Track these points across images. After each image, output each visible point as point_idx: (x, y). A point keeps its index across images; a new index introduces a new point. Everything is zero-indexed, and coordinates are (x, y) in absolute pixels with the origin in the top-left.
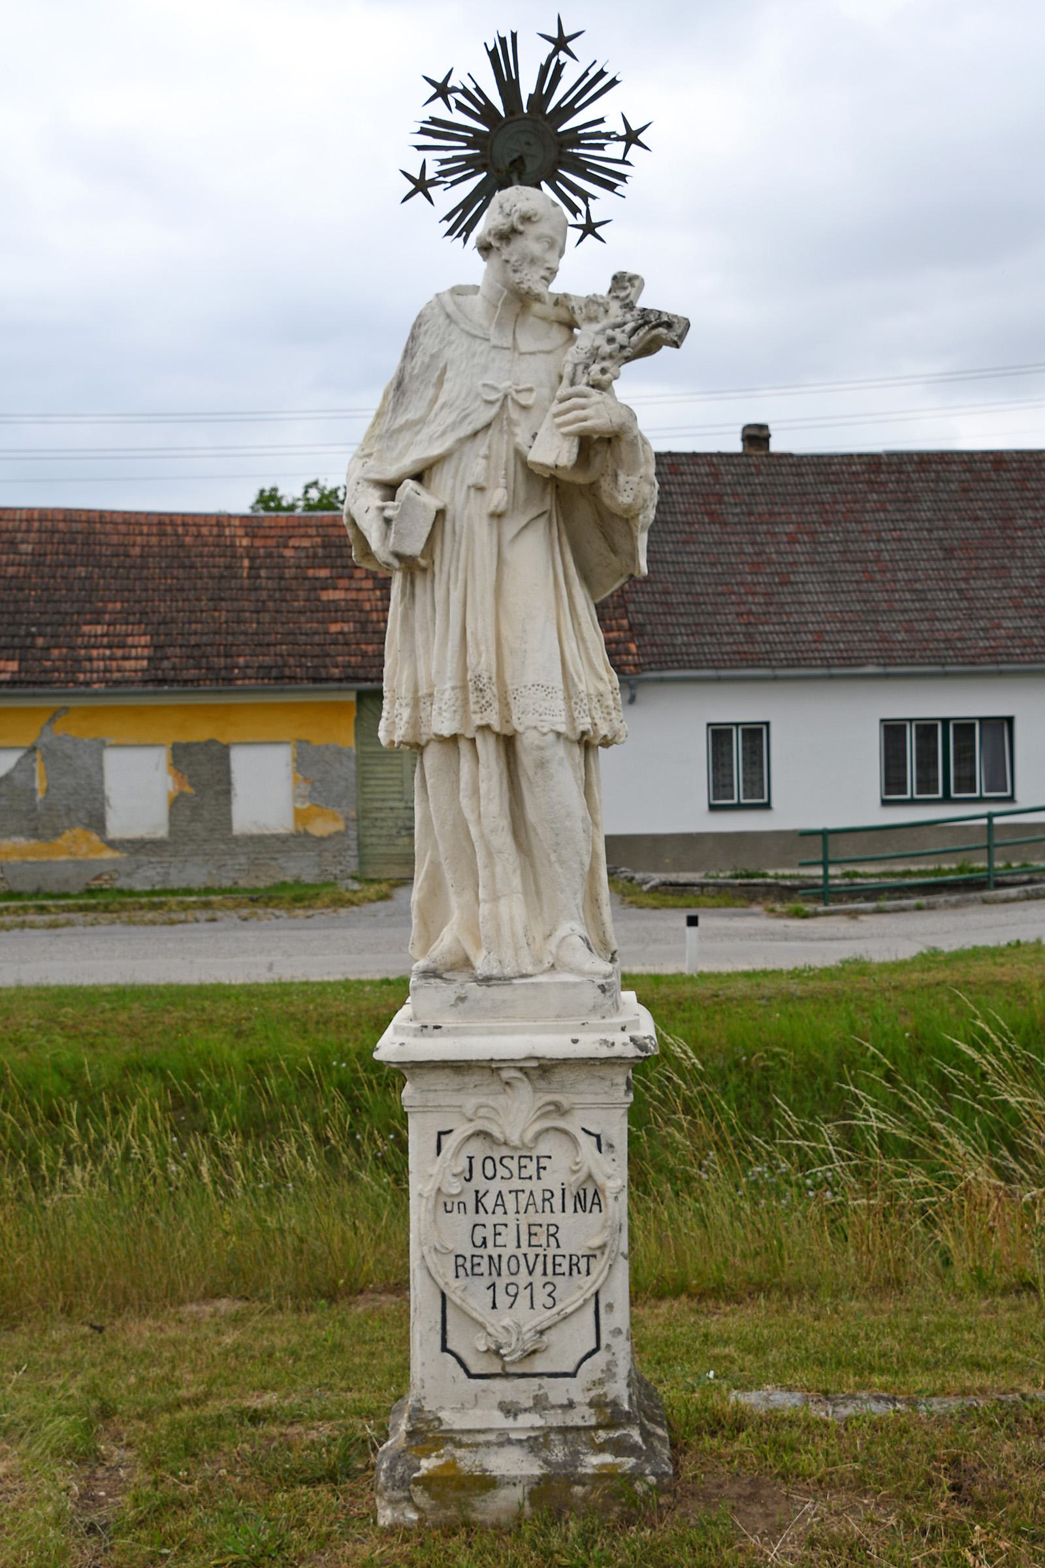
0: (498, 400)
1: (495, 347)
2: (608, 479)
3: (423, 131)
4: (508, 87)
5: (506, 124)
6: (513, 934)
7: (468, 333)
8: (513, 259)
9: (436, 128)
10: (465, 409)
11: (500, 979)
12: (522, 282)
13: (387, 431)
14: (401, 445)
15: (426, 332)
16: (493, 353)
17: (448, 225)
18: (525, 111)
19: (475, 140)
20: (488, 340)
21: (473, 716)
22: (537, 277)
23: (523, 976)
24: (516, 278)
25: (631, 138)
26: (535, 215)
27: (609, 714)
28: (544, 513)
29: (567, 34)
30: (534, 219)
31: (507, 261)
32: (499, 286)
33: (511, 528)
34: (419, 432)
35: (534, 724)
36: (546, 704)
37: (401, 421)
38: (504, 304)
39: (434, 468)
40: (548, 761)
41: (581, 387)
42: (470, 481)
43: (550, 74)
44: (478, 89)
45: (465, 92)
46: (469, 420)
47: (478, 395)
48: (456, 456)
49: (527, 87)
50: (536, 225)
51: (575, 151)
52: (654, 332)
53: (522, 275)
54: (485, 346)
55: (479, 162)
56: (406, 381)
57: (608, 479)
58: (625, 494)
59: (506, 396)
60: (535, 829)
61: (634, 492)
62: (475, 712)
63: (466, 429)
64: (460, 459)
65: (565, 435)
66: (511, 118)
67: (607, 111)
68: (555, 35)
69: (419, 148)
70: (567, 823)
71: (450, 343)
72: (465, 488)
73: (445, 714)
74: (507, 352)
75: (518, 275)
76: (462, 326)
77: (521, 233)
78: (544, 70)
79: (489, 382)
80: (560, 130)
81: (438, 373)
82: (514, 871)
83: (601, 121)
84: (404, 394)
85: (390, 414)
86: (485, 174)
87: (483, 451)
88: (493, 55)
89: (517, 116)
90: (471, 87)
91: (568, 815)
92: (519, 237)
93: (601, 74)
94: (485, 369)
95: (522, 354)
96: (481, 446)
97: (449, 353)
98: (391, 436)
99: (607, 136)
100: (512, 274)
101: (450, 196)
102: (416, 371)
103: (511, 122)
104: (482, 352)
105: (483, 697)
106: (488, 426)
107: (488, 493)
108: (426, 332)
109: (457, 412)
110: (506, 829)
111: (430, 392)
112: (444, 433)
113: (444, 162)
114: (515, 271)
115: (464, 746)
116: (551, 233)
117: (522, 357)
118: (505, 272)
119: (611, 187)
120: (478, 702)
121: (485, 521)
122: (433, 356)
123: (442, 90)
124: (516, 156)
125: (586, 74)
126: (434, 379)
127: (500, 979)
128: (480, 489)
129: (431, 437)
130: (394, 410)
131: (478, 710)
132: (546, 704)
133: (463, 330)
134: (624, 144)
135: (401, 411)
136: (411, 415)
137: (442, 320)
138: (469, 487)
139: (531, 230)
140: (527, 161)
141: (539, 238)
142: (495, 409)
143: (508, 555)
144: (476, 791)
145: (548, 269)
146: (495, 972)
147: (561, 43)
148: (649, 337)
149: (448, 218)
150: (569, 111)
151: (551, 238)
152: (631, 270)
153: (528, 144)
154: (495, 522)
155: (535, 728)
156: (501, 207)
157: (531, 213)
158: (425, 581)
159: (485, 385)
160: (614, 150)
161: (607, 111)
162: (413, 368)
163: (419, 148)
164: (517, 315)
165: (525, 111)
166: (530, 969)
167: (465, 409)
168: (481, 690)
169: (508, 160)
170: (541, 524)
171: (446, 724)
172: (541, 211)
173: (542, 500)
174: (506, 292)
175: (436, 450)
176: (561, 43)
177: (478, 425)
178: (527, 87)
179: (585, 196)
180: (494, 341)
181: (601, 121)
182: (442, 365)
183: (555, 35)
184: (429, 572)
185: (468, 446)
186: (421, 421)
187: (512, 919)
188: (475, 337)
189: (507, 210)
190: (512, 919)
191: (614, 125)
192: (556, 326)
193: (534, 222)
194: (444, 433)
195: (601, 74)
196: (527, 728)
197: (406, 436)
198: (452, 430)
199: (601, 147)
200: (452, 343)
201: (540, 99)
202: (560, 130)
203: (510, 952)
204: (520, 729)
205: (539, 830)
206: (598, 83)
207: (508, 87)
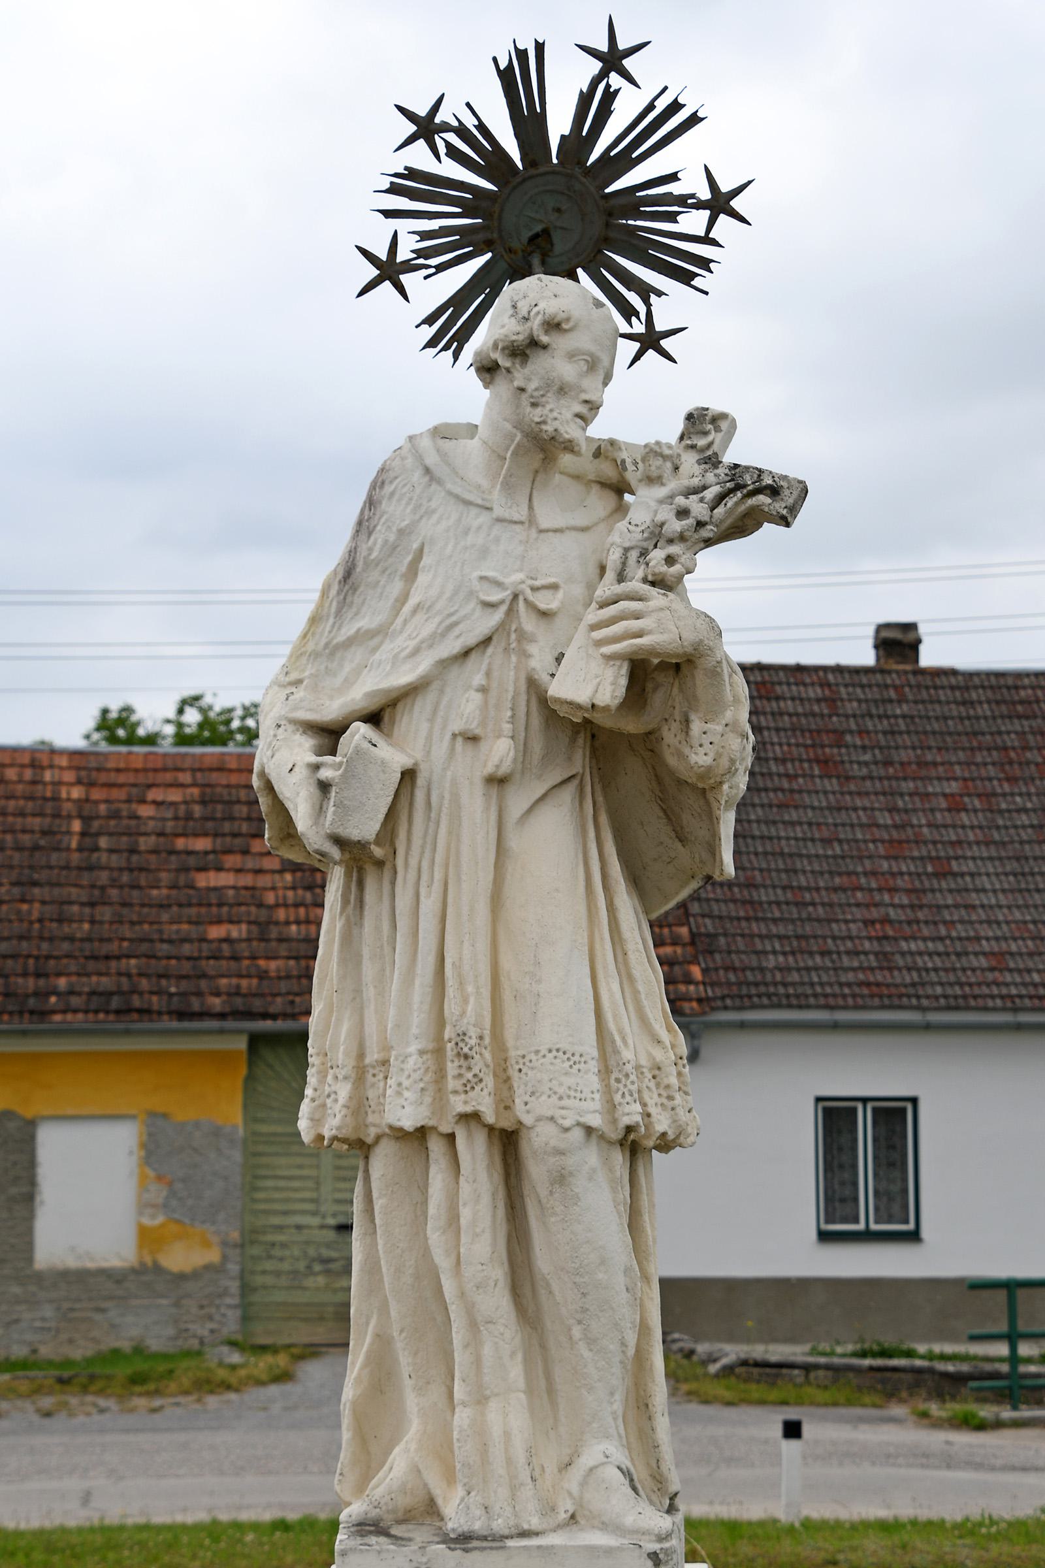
0: (502, 602)
1: (500, 520)
2: (675, 726)
3: (394, 190)
4: (529, 122)
5: (524, 180)
6: (509, 1461)
7: (457, 497)
9: (413, 183)
10: (451, 614)
11: (485, 1538)
12: (544, 422)
13: (327, 645)
14: (347, 668)
15: (392, 494)
16: (497, 530)
17: (429, 332)
18: (555, 161)
19: (474, 203)
20: (489, 509)
21: (452, 1098)
22: (568, 415)
23: (524, 1534)
24: (536, 415)
25: (720, 204)
26: (568, 320)
27: (670, 1098)
28: (573, 777)
29: (622, 45)
30: (565, 326)
31: (522, 390)
32: (508, 426)
33: (518, 801)
34: (375, 650)
35: (549, 1114)
36: (570, 1081)
37: (348, 630)
38: (515, 453)
39: (400, 706)
40: (571, 1174)
41: (635, 585)
42: (457, 726)
43: (595, 106)
44: (481, 127)
45: (462, 131)
46: (457, 631)
47: (471, 593)
48: (435, 685)
49: (559, 124)
51: (630, 222)
52: (751, 502)
53: (546, 411)
54: (484, 518)
55: (481, 237)
56: (358, 570)
57: (675, 726)
58: (701, 751)
59: (516, 596)
60: (548, 1285)
62: (455, 1092)
63: (453, 646)
64: (442, 691)
66: (532, 171)
67: (684, 162)
68: (604, 47)
69: (388, 214)
70: (600, 1276)
71: (430, 513)
72: (448, 736)
73: (407, 1094)
74: (518, 528)
75: (539, 411)
76: (449, 486)
77: (545, 347)
78: (585, 100)
79: (490, 574)
80: (607, 191)
81: (410, 558)
82: (513, 1354)
83: (673, 177)
84: (354, 589)
85: (331, 620)
86: (489, 255)
87: (478, 679)
88: (506, 76)
89: (542, 169)
90: (470, 122)
91: (603, 1262)
92: (542, 352)
93: (675, 107)
94: (484, 553)
95: (541, 531)
96: (475, 672)
97: (427, 528)
98: (332, 654)
99: (682, 200)
100: (529, 409)
101: (434, 289)
102: (372, 557)
103: (531, 177)
104: (479, 528)
105: (469, 1068)
106: (487, 641)
107: (484, 746)
108: (392, 494)
109: (437, 620)
110: (501, 1284)
111: (397, 587)
112: (416, 651)
113: (424, 235)
114: (534, 405)
115: (436, 1146)
117: (543, 535)
118: (518, 407)
119: (686, 278)
120: (460, 1076)
121: (479, 787)
122: (401, 532)
123: (426, 128)
124: (538, 228)
125: (651, 107)
126: (403, 568)
127: (485, 1538)
128: (473, 739)
129: (395, 657)
130: (338, 613)
131: (460, 1088)
132: (570, 1081)
133: (450, 493)
134: (707, 213)
135: (350, 615)
136: (365, 622)
137: (417, 476)
138: (454, 736)
139: (561, 343)
140: (557, 237)
141: (571, 356)
142: (498, 615)
143: (513, 842)
144: (453, 1219)
145: (586, 402)
146: (478, 1526)
147: (613, 59)
148: (742, 508)
149: (430, 320)
150: (622, 161)
151: (592, 355)
152: (716, 405)
153: (559, 210)
154: (494, 791)
155: (552, 1119)
156: (514, 307)
158: (380, 880)
159: (482, 578)
160: (693, 222)
161: (684, 162)
162: (371, 550)
163: (388, 214)
165: (555, 161)
166: (534, 1523)
167: (451, 614)
168: (466, 1057)
169: (526, 235)
170: (567, 795)
171: (408, 1109)
172: (576, 314)
173: (570, 759)
174: (519, 437)
175: (404, 677)
176: (613, 59)
177: (471, 639)
178: (559, 124)
179: (646, 291)
180: (498, 511)
181: (673, 177)
182: (415, 546)
183: (604, 47)
184: (388, 866)
185: (454, 672)
186: (381, 632)
187: (507, 1435)
188: (468, 503)
189: (524, 312)
190: (507, 1435)
191: (693, 184)
192: (596, 488)
193: (566, 331)
194: (416, 651)
195: (675, 107)
196: (539, 1119)
197: (357, 655)
198: (431, 646)
199: (672, 217)
200: (434, 511)
201: (578, 142)
202: (607, 191)
203: (503, 1492)
204: (527, 1120)
205: (555, 1287)
206: (668, 121)
207: (529, 122)
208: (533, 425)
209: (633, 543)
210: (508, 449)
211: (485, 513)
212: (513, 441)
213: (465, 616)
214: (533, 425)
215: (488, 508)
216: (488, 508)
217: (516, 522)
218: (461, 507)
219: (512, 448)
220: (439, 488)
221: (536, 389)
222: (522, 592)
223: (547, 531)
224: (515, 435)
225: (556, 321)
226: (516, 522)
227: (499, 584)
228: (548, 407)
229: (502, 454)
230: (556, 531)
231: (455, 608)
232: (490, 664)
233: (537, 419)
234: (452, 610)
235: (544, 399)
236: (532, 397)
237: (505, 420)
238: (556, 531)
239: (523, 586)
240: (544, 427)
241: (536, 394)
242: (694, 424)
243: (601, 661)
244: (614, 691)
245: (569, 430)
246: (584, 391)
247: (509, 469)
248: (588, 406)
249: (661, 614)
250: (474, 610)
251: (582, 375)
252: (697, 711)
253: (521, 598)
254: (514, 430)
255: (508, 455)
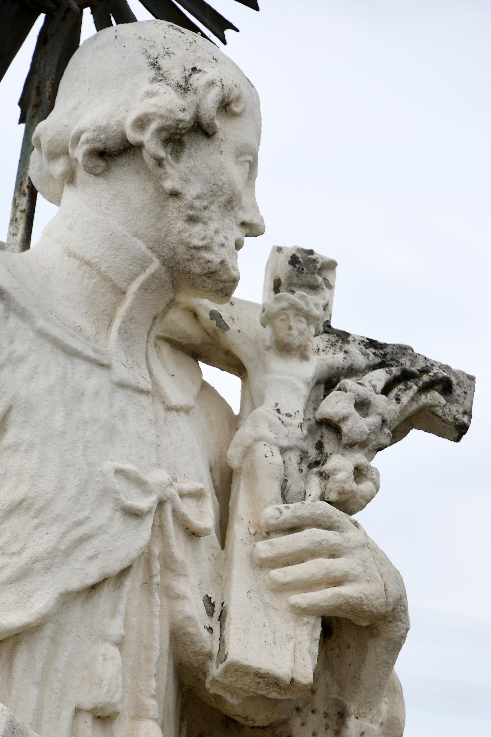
1: (122, 385)
2: (315, 722)
7: (56, 342)
8: (191, 191)
10: (79, 523)
12: (207, 248)
24: (196, 235)
31: (175, 194)
32: (141, 246)
38: (145, 288)
46: (89, 549)
47: (106, 493)
48: (48, 631)
52: (424, 399)
53: (210, 233)
54: (96, 380)
59: (161, 504)
64: (54, 641)
65: (300, 612)
72: (68, 713)
75: (198, 229)
76: (40, 323)
87: (116, 627)
92: (203, 142)
94: (111, 433)
96: (113, 616)
100: (180, 225)
109: (57, 529)
112: (22, 576)
114: (192, 220)
118: (159, 218)
133: (42, 334)
138: (78, 711)
148: (415, 407)
152: (323, 251)
159: (119, 472)
167: (79, 523)
174: (156, 264)
180: (121, 372)
185: (77, 612)
188: (72, 353)
192: (166, 349)
194: (22, 576)
198: (47, 569)
200: (21, 359)
208: (181, 249)
209: (293, 442)
210: (132, 278)
211: (99, 371)
212: (143, 268)
213: (101, 527)
214: (181, 249)
215: (102, 365)
216: (102, 365)
218: (61, 358)
219: (142, 278)
220: (22, 324)
221: (198, 197)
222: (171, 499)
224: (151, 261)
227: (140, 484)
228: (213, 226)
229: (122, 284)
231: (86, 513)
233: (196, 242)
234: (81, 516)
235: (206, 214)
236: (192, 207)
237: (135, 235)
240: (207, 255)
241: (197, 204)
242: (300, 271)
243: (288, 616)
247: (131, 309)
250: (111, 519)
253: (168, 508)
254: (149, 253)
255: (134, 287)
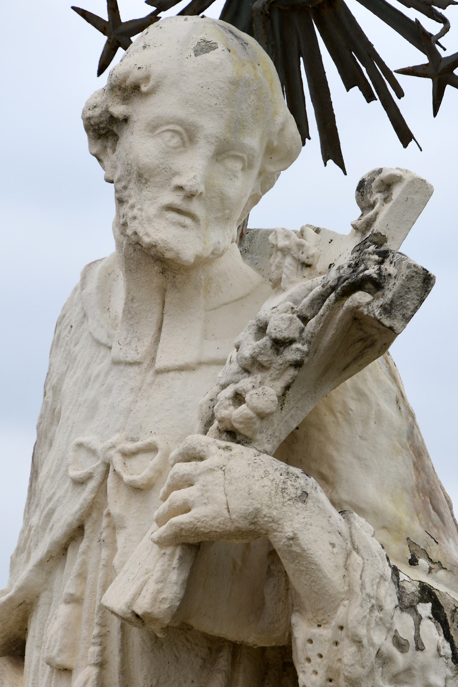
0: (90, 477)
1: (116, 363)
22: (151, 210)
26: (147, 78)
50: (154, 100)
52: (349, 302)
61: (325, 661)
74: (133, 371)
77: (126, 120)
95: (159, 372)
116: (181, 113)
117: (160, 378)
139: (143, 112)
141: (153, 128)
145: (180, 188)
151: (180, 122)
157: (136, 75)
159: (80, 445)
164: (163, 292)
172: (157, 70)
193: (147, 94)
217: (131, 364)
223: (167, 370)
225: (130, 81)
226: (131, 364)
230: (181, 369)
232: (84, 563)
238: (181, 369)
239: (112, 452)
244: (159, 592)
245: (150, 230)
246: (176, 174)
248: (181, 194)
249: (210, 478)
251: (169, 152)
252: (301, 610)
